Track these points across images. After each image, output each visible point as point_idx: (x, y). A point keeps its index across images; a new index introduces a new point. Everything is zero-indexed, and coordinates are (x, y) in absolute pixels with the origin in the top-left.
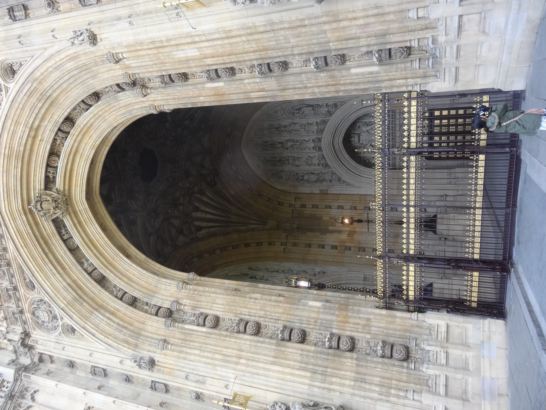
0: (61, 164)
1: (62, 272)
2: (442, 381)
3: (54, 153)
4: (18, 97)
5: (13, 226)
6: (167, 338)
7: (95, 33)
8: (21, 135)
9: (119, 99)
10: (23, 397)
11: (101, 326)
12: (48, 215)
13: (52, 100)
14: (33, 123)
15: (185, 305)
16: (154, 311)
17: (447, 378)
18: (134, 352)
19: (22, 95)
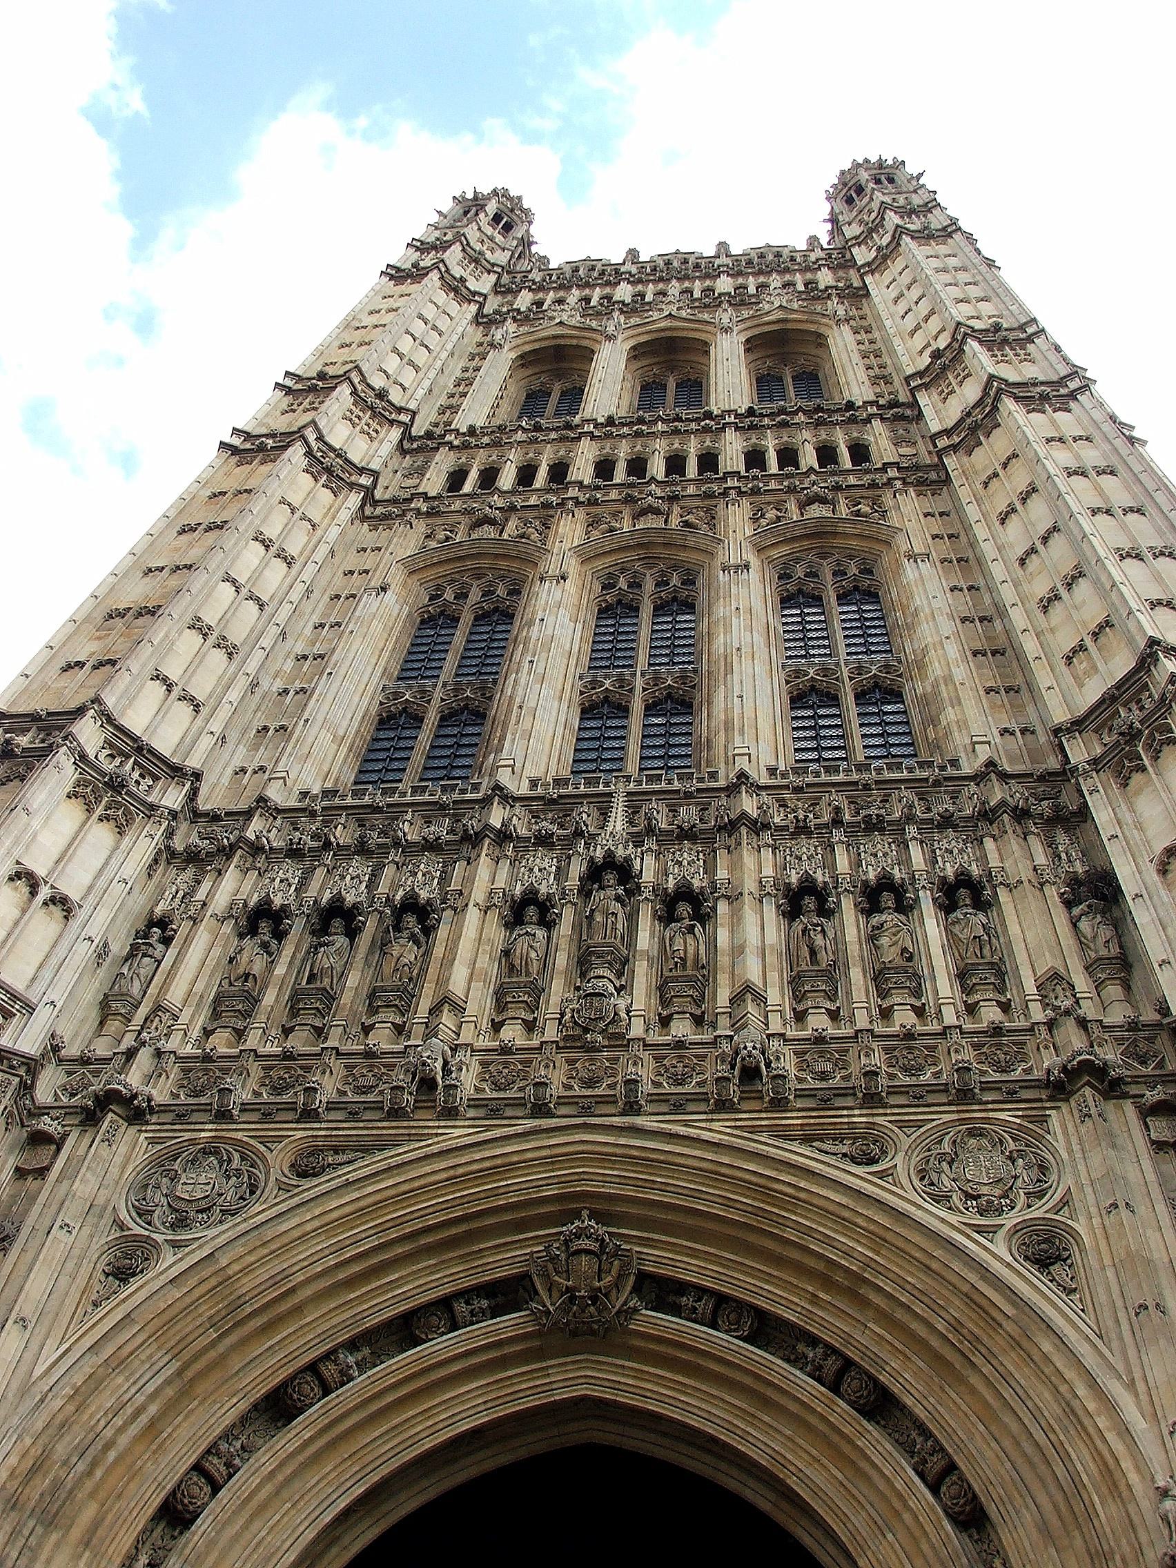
0: (723, 1341)
4: (965, 1264)
5: (529, 1155)
8: (835, 1244)
11: (120, 1380)
12: (550, 1266)
13: (957, 1366)
14: (879, 1289)
19: (973, 1277)
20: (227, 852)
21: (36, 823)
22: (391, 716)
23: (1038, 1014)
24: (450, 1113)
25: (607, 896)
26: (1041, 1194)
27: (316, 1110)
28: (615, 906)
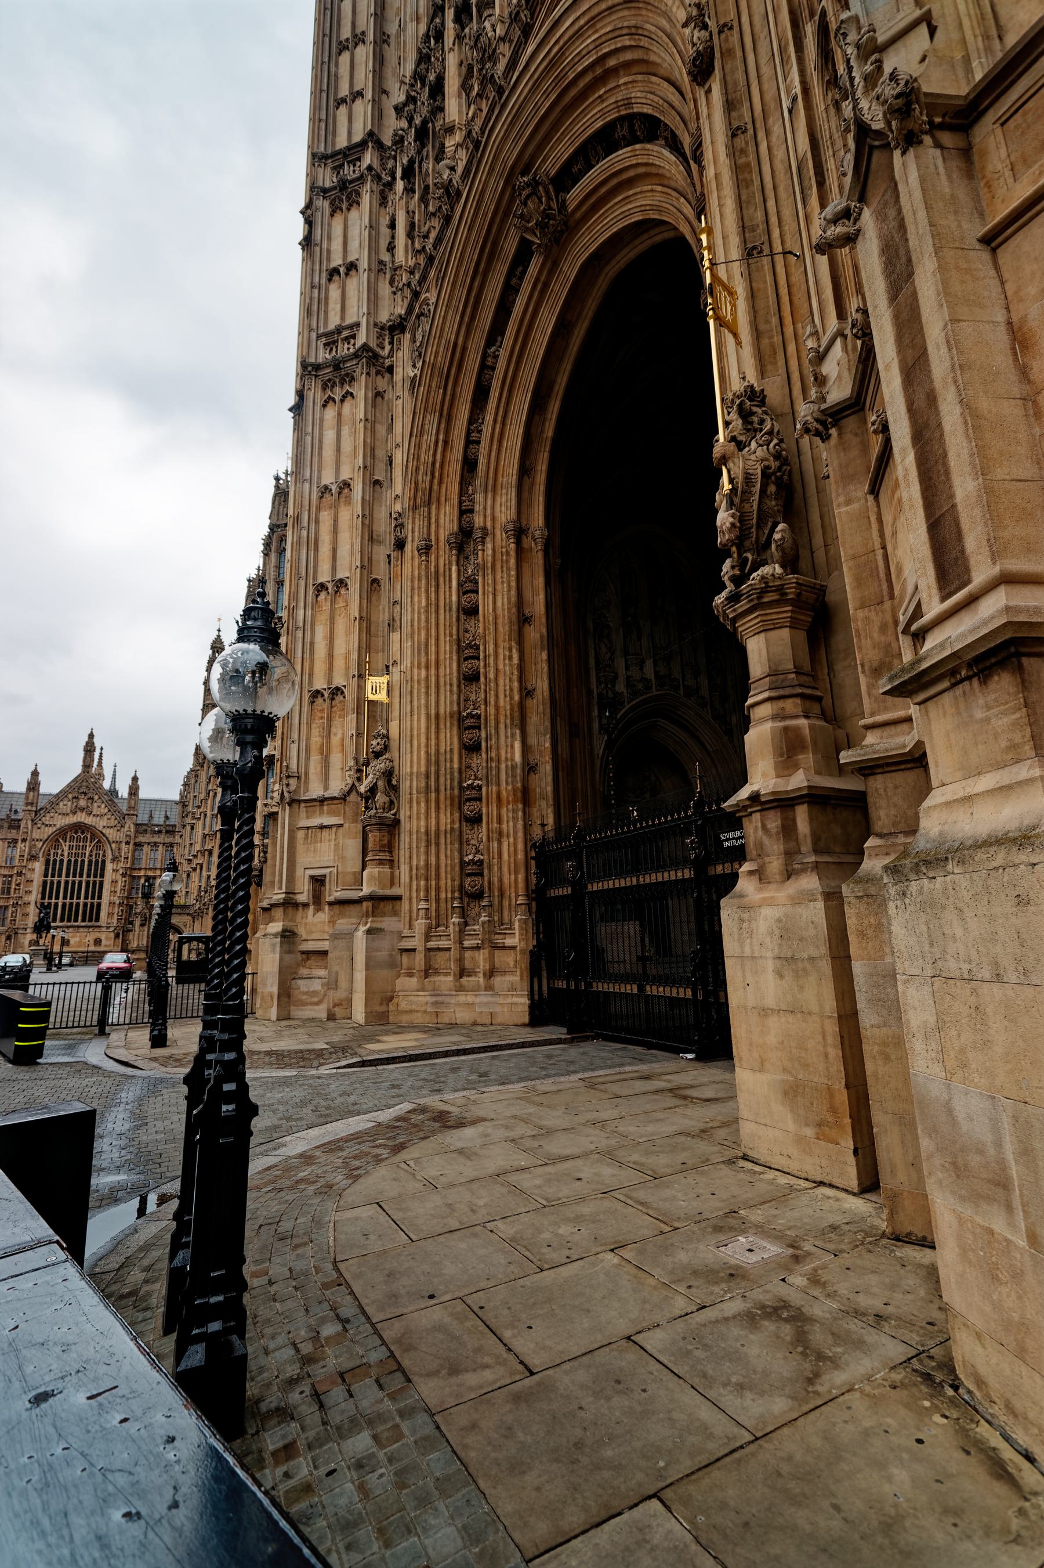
1: (466, 319)
2: (443, 943)
17: (449, 949)
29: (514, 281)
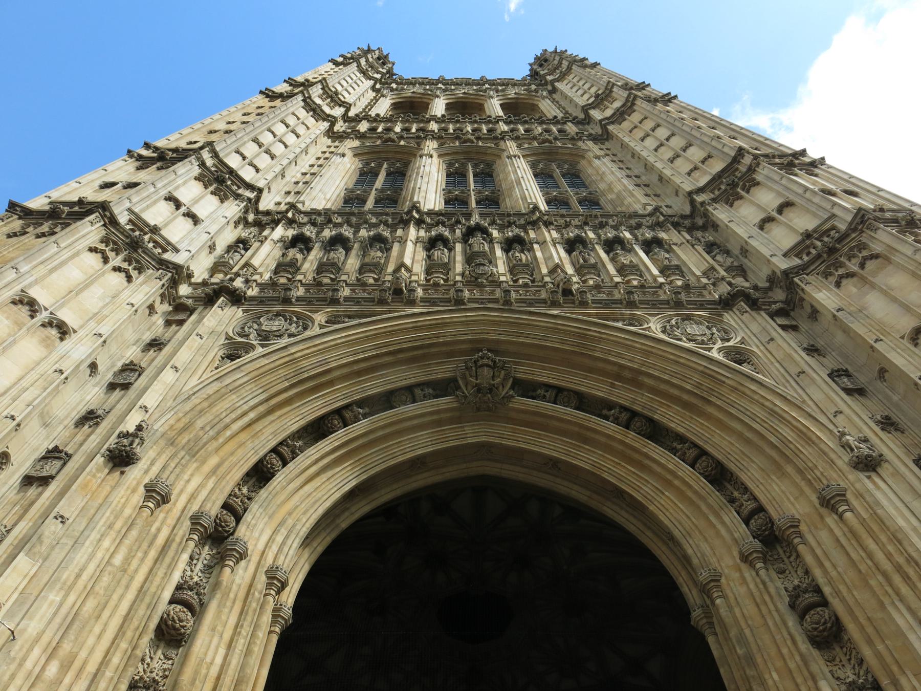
0: (561, 410)
3: (582, 402)
6: (167, 506)
7: (879, 470)
9: (722, 514)
10: (128, 260)
11: (234, 397)
15: (232, 571)
16: (237, 503)
18: (158, 434)
20: (276, 223)
21: (180, 181)
22: (350, 199)
23: (705, 281)
24: (412, 303)
25: (478, 242)
26: (728, 340)
27: (338, 299)
28: (482, 241)
29: (418, 392)
